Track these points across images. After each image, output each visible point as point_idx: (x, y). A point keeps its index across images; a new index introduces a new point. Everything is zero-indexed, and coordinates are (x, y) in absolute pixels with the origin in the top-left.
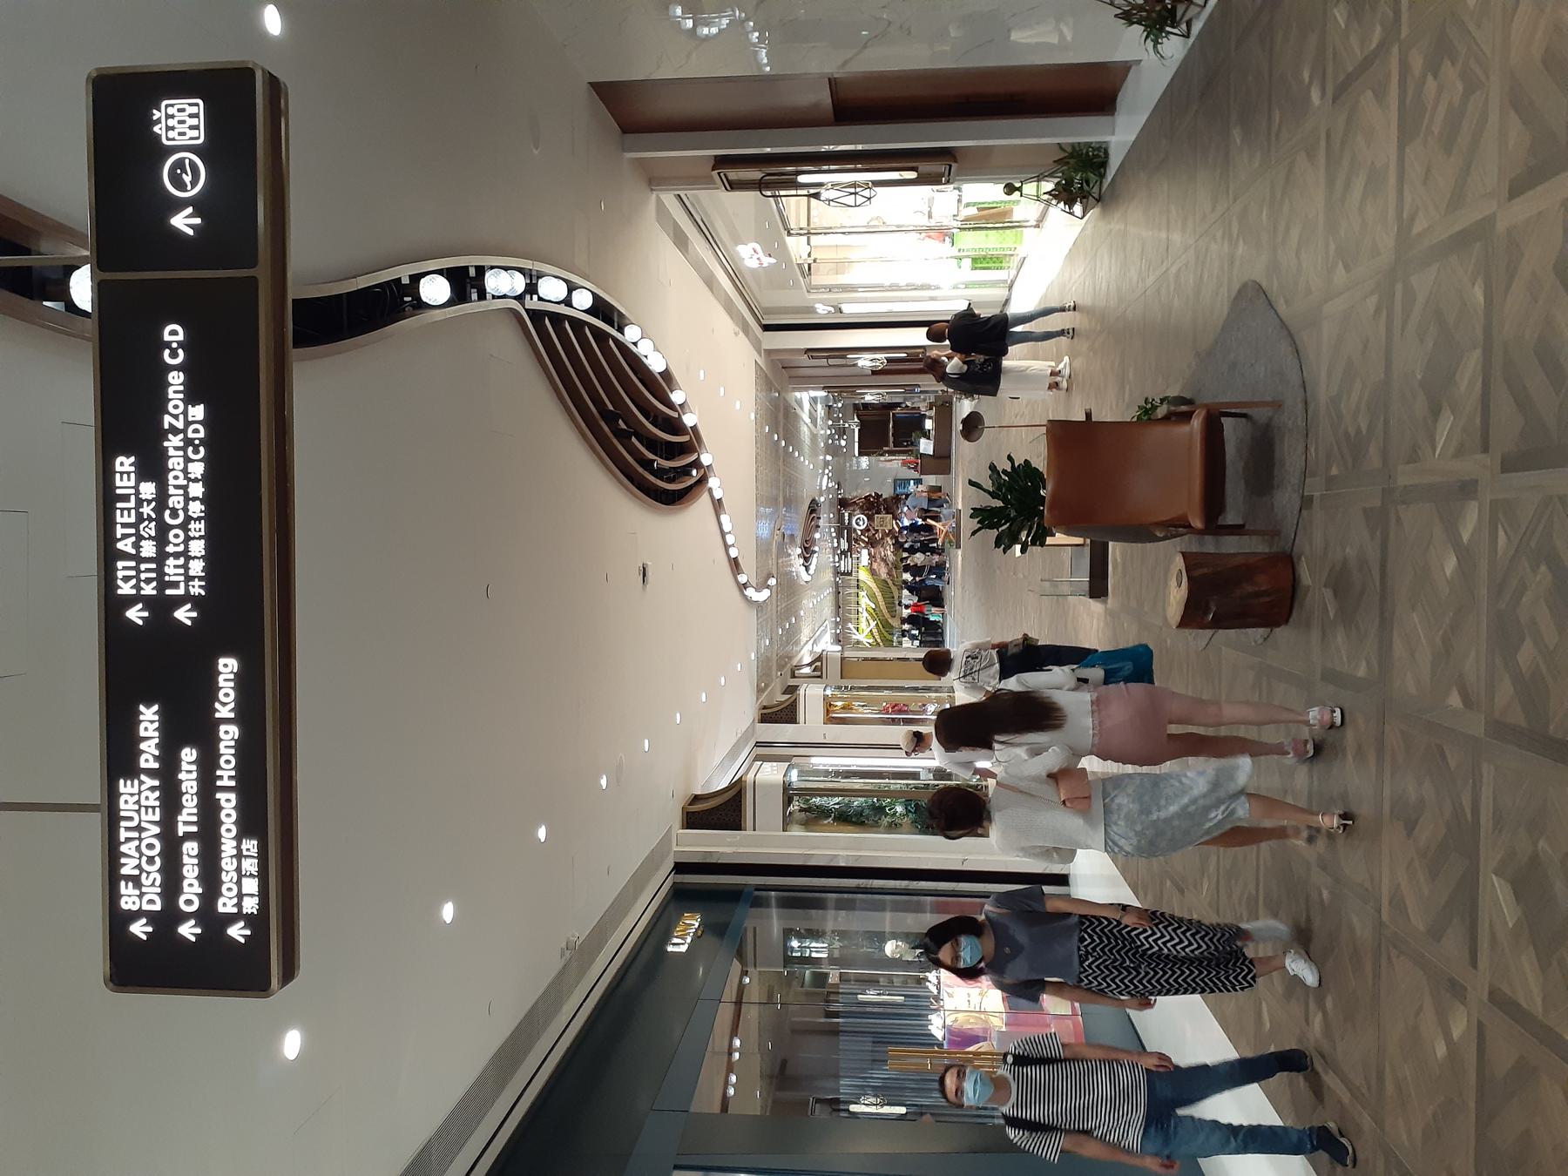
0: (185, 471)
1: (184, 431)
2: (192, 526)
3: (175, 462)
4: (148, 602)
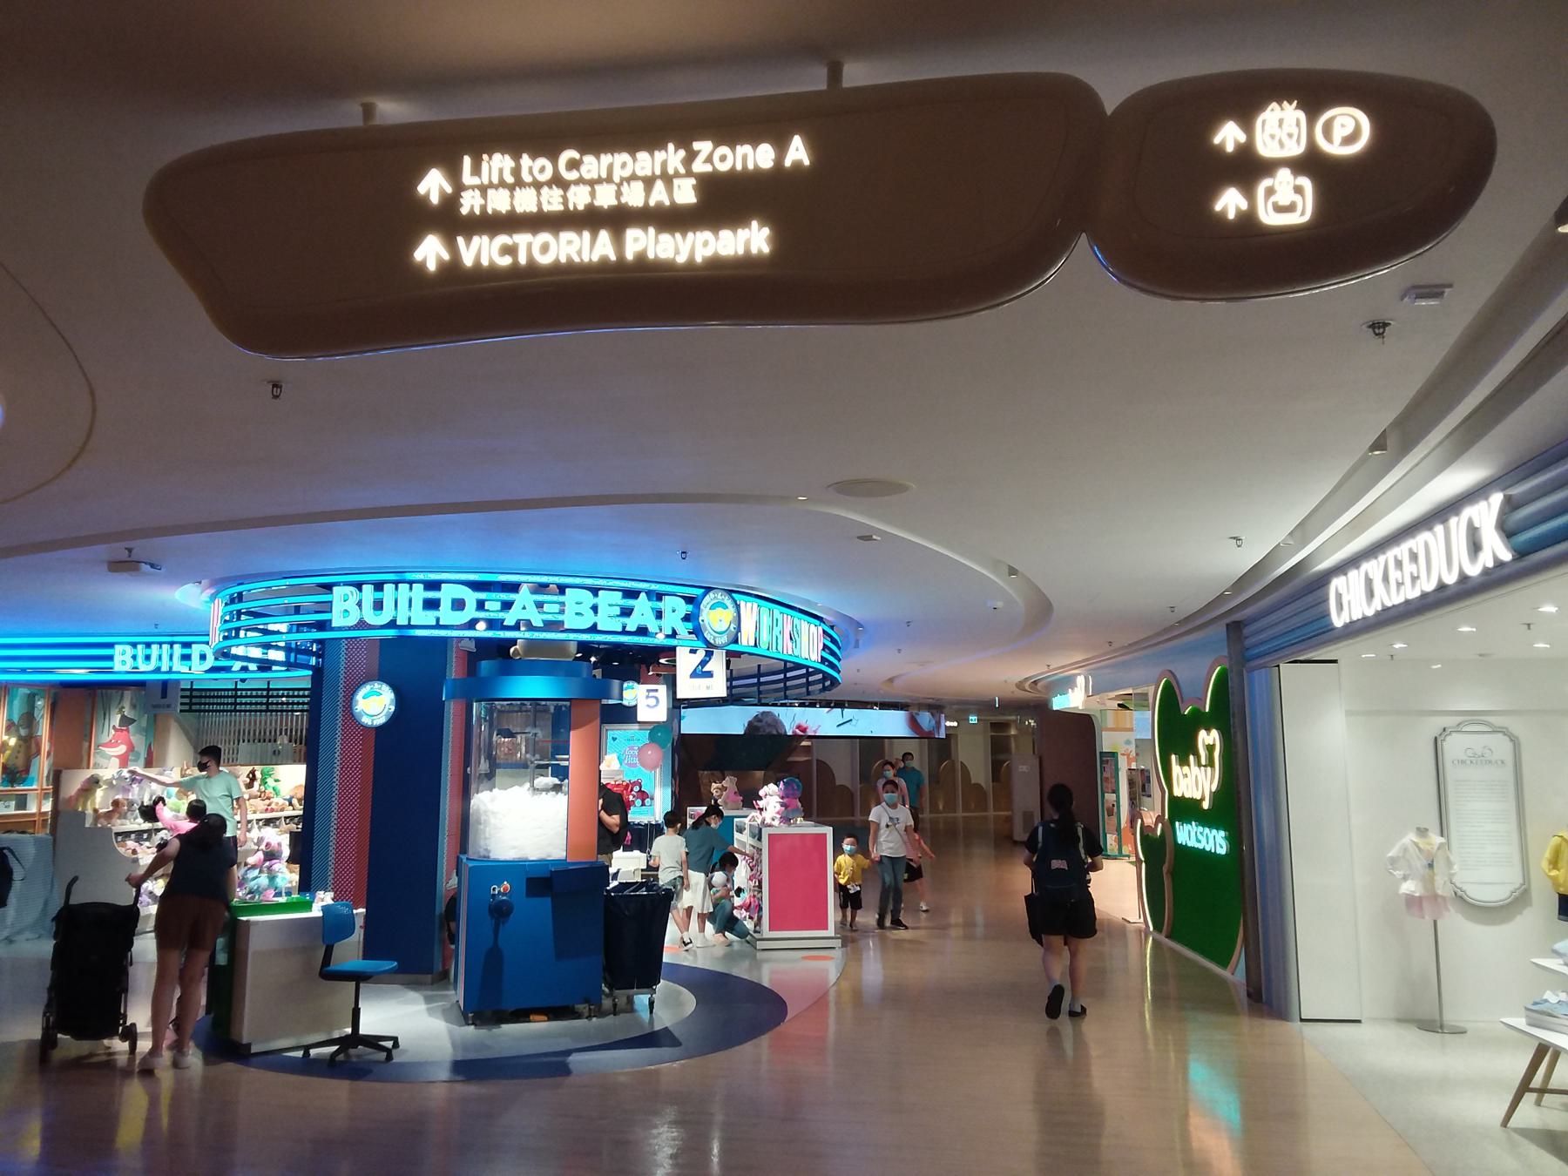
0: (634, 177)
2: (557, 192)
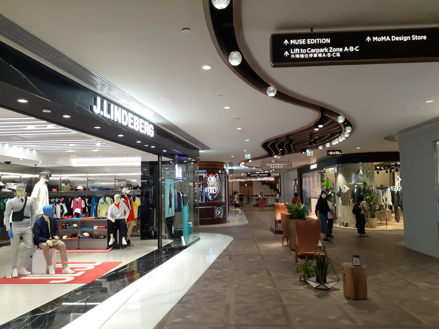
0: (319, 53)
1: (329, 52)
2: (307, 55)
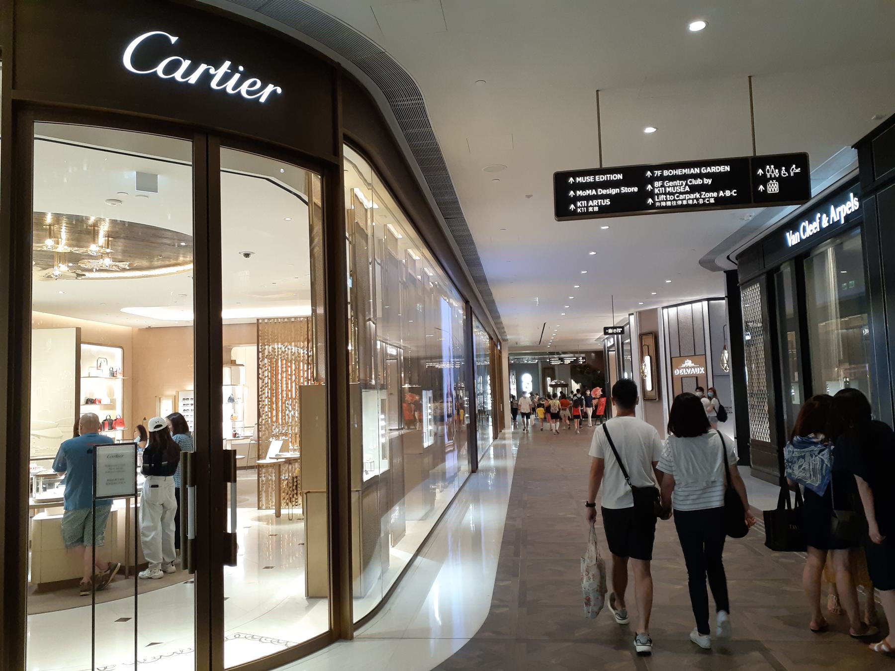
3: (692, 196)
4: (652, 191)
